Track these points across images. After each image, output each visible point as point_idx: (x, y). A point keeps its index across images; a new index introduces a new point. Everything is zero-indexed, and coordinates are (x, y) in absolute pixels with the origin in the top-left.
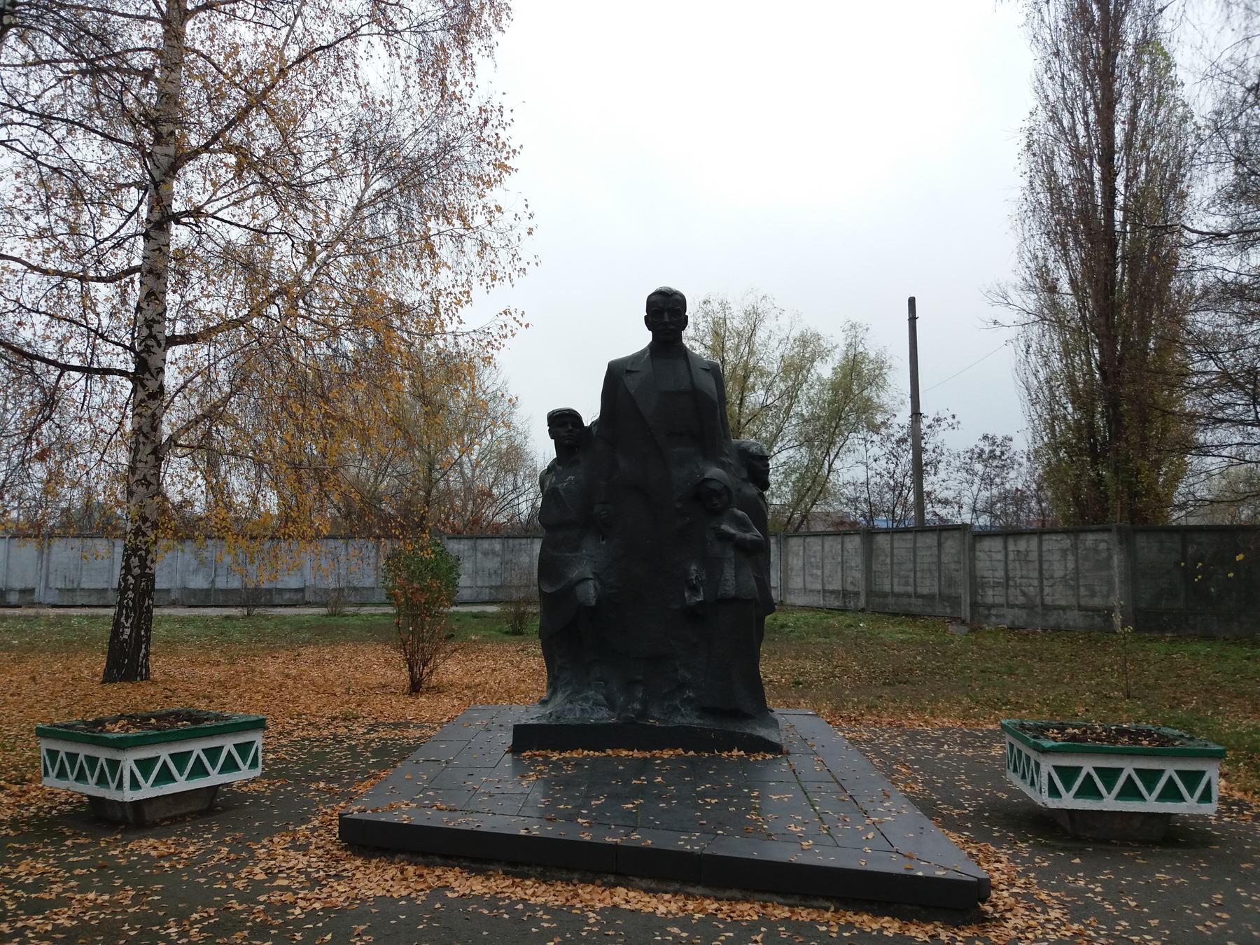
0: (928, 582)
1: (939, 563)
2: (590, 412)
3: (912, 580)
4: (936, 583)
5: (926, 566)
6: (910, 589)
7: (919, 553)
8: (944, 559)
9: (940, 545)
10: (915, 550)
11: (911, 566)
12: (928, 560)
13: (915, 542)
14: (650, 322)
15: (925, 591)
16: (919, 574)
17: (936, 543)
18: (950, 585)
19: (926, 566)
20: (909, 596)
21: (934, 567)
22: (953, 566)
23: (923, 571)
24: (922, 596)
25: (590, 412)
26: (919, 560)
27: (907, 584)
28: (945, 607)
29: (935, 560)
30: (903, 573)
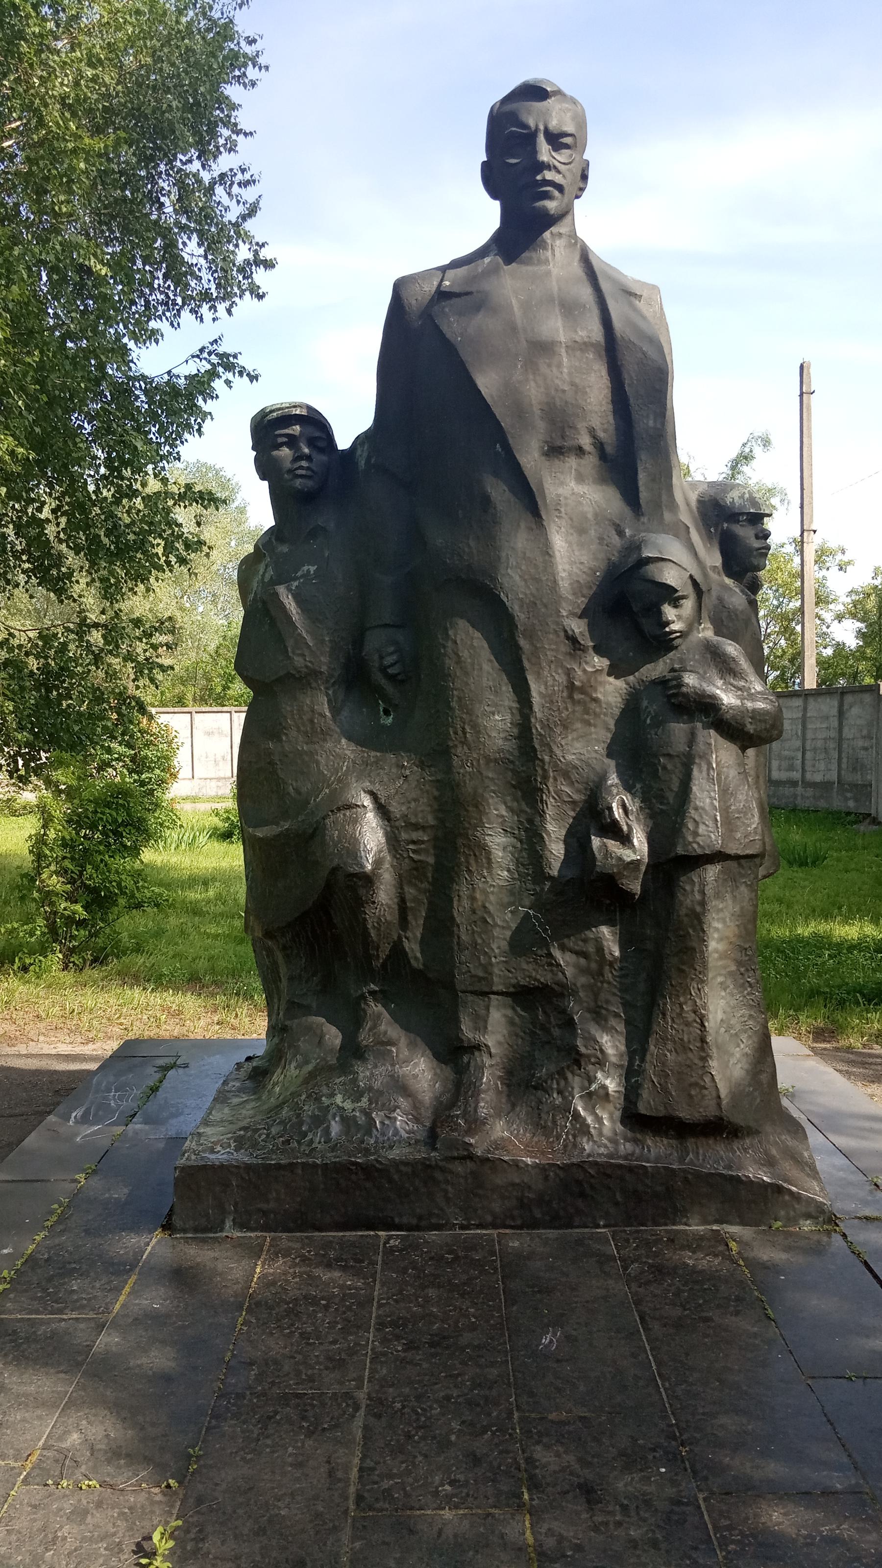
0: (822, 766)
1: (840, 740)
2: (351, 416)
3: (799, 762)
4: (834, 766)
5: (820, 744)
6: (796, 775)
7: (810, 726)
8: (847, 733)
9: (841, 714)
10: (804, 720)
11: (799, 743)
12: (821, 735)
13: (805, 709)
14: (494, 178)
15: (818, 778)
16: (809, 755)
17: (835, 711)
18: (854, 769)
19: (820, 744)
20: (793, 783)
21: (832, 745)
22: (860, 743)
23: (815, 750)
24: (813, 785)
25: (351, 416)
26: (809, 735)
27: (791, 768)
28: (846, 799)
29: (833, 734)
30: (786, 753)
